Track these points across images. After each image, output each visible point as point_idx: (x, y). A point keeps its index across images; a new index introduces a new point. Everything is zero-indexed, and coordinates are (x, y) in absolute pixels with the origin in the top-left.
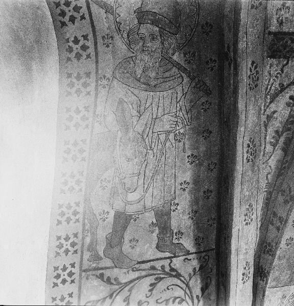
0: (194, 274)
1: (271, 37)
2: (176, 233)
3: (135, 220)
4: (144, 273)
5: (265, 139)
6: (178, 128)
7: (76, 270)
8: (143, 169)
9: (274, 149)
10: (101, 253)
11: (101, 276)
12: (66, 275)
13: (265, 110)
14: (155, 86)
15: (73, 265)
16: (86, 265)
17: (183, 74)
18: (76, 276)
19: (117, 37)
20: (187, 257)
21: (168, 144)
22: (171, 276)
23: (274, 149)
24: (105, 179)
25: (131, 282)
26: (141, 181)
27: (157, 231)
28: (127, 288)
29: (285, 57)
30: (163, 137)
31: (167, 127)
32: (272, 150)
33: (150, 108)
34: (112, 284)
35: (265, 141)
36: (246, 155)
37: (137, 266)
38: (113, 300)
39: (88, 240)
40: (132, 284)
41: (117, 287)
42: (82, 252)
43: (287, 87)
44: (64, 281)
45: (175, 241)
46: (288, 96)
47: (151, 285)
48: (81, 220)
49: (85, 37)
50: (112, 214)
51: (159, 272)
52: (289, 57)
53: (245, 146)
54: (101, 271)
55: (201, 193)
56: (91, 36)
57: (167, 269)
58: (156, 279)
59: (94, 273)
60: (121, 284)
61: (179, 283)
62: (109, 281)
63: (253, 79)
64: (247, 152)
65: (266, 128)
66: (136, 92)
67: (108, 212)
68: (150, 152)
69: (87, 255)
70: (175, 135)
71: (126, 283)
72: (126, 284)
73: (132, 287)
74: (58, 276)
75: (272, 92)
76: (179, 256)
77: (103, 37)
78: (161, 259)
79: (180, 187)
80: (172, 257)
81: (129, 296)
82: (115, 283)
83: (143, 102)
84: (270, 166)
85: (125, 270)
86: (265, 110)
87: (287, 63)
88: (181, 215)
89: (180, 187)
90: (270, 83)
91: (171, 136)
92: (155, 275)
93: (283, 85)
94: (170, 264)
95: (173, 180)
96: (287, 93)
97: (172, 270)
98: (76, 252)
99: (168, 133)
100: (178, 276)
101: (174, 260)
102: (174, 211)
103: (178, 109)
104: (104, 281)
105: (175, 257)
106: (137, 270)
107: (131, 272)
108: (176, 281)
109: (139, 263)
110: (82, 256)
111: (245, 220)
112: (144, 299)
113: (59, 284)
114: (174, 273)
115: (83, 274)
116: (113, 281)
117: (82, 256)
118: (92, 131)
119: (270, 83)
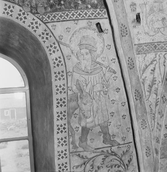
0: (124, 154)
1: (136, 46)
2: (112, 136)
3: (91, 130)
4: (98, 154)
5: (144, 89)
6: (104, 89)
7: (67, 152)
8: (92, 108)
9: (150, 93)
10: (78, 145)
11: (79, 155)
12: (63, 155)
13: (141, 77)
14: (91, 73)
15: (66, 150)
16: (71, 150)
17: (102, 66)
18: (68, 155)
19: (72, 55)
20: (119, 146)
21: (101, 96)
22: (113, 155)
23: (150, 93)
24: (76, 114)
25: (93, 158)
26: (92, 114)
27: (102, 135)
28: (91, 160)
29: (144, 53)
30: (98, 93)
31: (99, 89)
32: (149, 94)
33: (91, 82)
34: (84, 158)
35: (144, 90)
36: (134, 98)
37: (95, 151)
38: (86, 166)
39: (71, 140)
40: (94, 159)
41: (87, 160)
42: (69, 145)
43: (149, 66)
44: (62, 157)
45: (113, 139)
46: (150, 70)
47: (103, 159)
48: (67, 131)
49: (60, 58)
50: (80, 129)
51: (106, 153)
52: (146, 53)
53: (134, 93)
54: (79, 153)
55: (121, 117)
56: (62, 57)
57: (110, 152)
58: (105, 156)
59: (75, 154)
60: (88, 158)
61: (117, 158)
62: (82, 157)
63: (131, 64)
64: (135, 96)
65: (144, 85)
66: (83, 76)
67: (79, 128)
68: (94, 100)
69: (71, 146)
70: (103, 92)
71: (90, 158)
72: (91, 159)
73: (94, 160)
74: (60, 155)
75: (142, 69)
76: (115, 146)
77: (67, 57)
78: (106, 147)
79: (110, 115)
80: (111, 146)
81: (93, 164)
82: (85, 158)
83: (87, 80)
84: (150, 101)
85: (89, 153)
86: (141, 77)
87: (146, 56)
88: (113, 127)
89: (110, 115)
90: (141, 65)
91: (102, 93)
92: (104, 154)
93: (146, 65)
94: (111, 150)
95: (107, 112)
96: (149, 68)
97: (112, 152)
98: (66, 145)
99: (100, 91)
100: (115, 155)
101: (113, 148)
102: (109, 125)
103: (103, 81)
104: (80, 157)
105: (113, 146)
106: (95, 153)
107: (92, 153)
108: (114, 157)
109: (96, 149)
110: (69, 147)
111: (142, 127)
112: (100, 165)
113: (60, 158)
114: (113, 154)
115: (71, 154)
116: (84, 157)
117: (69, 147)
118: (67, 94)
119: (141, 65)
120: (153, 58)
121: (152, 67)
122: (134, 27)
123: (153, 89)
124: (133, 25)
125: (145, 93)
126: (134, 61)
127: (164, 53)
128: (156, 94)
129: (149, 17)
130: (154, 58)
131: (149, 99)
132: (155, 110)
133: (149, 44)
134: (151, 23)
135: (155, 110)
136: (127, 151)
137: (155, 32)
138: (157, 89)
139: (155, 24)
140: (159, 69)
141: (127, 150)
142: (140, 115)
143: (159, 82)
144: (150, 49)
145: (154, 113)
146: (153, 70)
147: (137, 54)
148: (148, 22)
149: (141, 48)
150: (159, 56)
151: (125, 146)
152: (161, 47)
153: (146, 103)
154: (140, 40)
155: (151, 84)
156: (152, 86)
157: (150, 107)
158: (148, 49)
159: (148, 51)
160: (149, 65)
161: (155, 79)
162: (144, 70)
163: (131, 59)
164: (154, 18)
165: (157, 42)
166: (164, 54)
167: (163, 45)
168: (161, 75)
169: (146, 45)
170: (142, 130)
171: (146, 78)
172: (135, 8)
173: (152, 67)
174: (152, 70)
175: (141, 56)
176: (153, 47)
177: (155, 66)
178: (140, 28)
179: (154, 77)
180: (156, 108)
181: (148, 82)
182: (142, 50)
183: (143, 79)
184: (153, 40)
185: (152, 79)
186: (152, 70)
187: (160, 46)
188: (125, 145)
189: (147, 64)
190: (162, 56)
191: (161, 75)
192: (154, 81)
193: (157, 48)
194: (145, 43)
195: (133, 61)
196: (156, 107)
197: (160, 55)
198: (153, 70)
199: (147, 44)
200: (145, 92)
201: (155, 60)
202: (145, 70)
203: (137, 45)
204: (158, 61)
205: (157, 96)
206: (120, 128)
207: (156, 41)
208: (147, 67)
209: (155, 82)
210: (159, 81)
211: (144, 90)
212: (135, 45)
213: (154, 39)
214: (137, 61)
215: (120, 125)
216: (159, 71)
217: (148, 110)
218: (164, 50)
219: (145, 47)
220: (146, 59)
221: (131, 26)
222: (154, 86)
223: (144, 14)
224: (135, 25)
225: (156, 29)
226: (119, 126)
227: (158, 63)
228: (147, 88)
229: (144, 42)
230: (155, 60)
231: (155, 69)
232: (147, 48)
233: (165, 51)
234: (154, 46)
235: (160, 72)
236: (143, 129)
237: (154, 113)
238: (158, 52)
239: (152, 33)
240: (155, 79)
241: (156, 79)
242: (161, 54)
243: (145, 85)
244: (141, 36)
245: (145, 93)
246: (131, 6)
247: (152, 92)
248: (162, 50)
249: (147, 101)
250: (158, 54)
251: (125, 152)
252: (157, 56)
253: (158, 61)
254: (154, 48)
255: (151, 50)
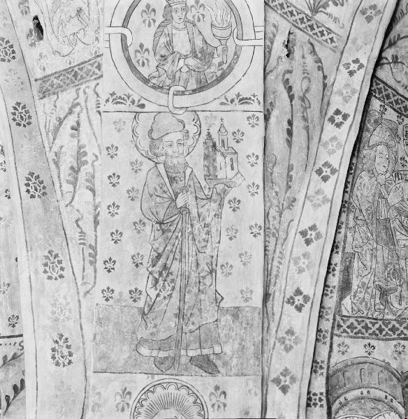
1: (39, 82)
9: (75, 188)
13: (51, 148)
23: (75, 188)
29: (54, 93)
32: (72, 189)
35: (60, 180)
43: (64, 119)
46: (68, 127)
75: (51, 128)
84: (78, 210)
86: (51, 148)
87: (58, 97)
90: (48, 121)
111: (45, 272)
119: (48, 121)
120: (71, 100)
121: (71, 121)
122: (32, 45)
123: (82, 176)
124: (30, 42)
125: (61, 186)
126: (32, 113)
127: (93, 84)
128: (93, 190)
129: (54, 18)
130: (75, 99)
131: (72, 204)
132: (96, 236)
133: (64, 73)
134: (60, 28)
135: (96, 236)
136: (15, 357)
137: (70, 44)
138: (93, 177)
139: (67, 27)
140: (88, 124)
141: (15, 354)
142: (41, 236)
143: (94, 158)
144: (65, 83)
145: (94, 244)
146: (76, 128)
147: (41, 99)
148: (55, 29)
149: (48, 84)
150: (85, 93)
151: (13, 343)
152: (85, 72)
153: (64, 215)
154: (46, 69)
155: (75, 165)
156: (79, 169)
157: (78, 226)
158: (61, 83)
159: (62, 86)
160: (66, 116)
161: (82, 151)
162: (56, 130)
163: (24, 107)
164: (63, 17)
165: (79, 65)
166: (94, 86)
167: (90, 67)
168: (96, 139)
169: (57, 75)
170: (47, 281)
171: (63, 149)
172: (28, 7)
173: (71, 121)
174: (73, 128)
175: (48, 101)
176: (70, 76)
177: (78, 117)
178: (42, 46)
179: (81, 143)
180: (96, 231)
181: (68, 160)
182: (49, 88)
183: (56, 153)
184: (70, 64)
185: (76, 148)
186: (73, 128)
187: (85, 70)
188: (13, 340)
189: (62, 117)
190: (90, 92)
191: (96, 139)
192: (80, 154)
193: (79, 77)
194: (56, 73)
195: (27, 112)
196: (96, 228)
197: (87, 90)
198: (76, 128)
199: (58, 74)
200: (60, 183)
201: (78, 104)
202: (58, 131)
203: (40, 79)
204: (83, 104)
205: (94, 195)
206: (6, 292)
207: (76, 64)
208: (61, 122)
209: (83, 159)
210: (94, 154)
211: (60, 180)
212: (36, 80)
213: (72, 61)
214: (40, 113)
215: (9, 285)
216: (88, 130)
217: (73, 233)
218: (92, 78)
219: (55, 81)
220: (58, 104)
221: (25, 44)
222: (82, 169)
223: (47, 15)
224: (33, 41)
225: (71, 37)
226: (6, 288)
227: (85, 111)
228: (67, 174)
229: (54, 71)
230: (78, 104)
231: (78, 124)
232: (59, 82)
233: (95, 79)
234: (73, 73)
235: (93, 129)
236: (50, 278)
237: (94, 244)
238: (81, 84)
239: (66, 49)
240: (82, 151)
241: (86, 149)
242: (88, 87)
243: (62, 168)
244: (47, 61)
245: (61, 186)
246: (21, 6)
247: (80, 184)
248: (88, 78)
249: (69, 208)
250: (82, 89)
251: (9, 357)
252: (81, 92)
253: (83, 104)
254: (73, 79)
255: (67, 85)
